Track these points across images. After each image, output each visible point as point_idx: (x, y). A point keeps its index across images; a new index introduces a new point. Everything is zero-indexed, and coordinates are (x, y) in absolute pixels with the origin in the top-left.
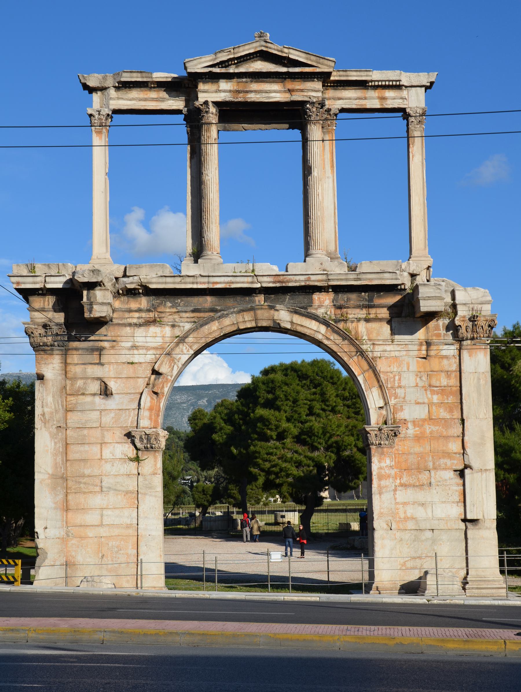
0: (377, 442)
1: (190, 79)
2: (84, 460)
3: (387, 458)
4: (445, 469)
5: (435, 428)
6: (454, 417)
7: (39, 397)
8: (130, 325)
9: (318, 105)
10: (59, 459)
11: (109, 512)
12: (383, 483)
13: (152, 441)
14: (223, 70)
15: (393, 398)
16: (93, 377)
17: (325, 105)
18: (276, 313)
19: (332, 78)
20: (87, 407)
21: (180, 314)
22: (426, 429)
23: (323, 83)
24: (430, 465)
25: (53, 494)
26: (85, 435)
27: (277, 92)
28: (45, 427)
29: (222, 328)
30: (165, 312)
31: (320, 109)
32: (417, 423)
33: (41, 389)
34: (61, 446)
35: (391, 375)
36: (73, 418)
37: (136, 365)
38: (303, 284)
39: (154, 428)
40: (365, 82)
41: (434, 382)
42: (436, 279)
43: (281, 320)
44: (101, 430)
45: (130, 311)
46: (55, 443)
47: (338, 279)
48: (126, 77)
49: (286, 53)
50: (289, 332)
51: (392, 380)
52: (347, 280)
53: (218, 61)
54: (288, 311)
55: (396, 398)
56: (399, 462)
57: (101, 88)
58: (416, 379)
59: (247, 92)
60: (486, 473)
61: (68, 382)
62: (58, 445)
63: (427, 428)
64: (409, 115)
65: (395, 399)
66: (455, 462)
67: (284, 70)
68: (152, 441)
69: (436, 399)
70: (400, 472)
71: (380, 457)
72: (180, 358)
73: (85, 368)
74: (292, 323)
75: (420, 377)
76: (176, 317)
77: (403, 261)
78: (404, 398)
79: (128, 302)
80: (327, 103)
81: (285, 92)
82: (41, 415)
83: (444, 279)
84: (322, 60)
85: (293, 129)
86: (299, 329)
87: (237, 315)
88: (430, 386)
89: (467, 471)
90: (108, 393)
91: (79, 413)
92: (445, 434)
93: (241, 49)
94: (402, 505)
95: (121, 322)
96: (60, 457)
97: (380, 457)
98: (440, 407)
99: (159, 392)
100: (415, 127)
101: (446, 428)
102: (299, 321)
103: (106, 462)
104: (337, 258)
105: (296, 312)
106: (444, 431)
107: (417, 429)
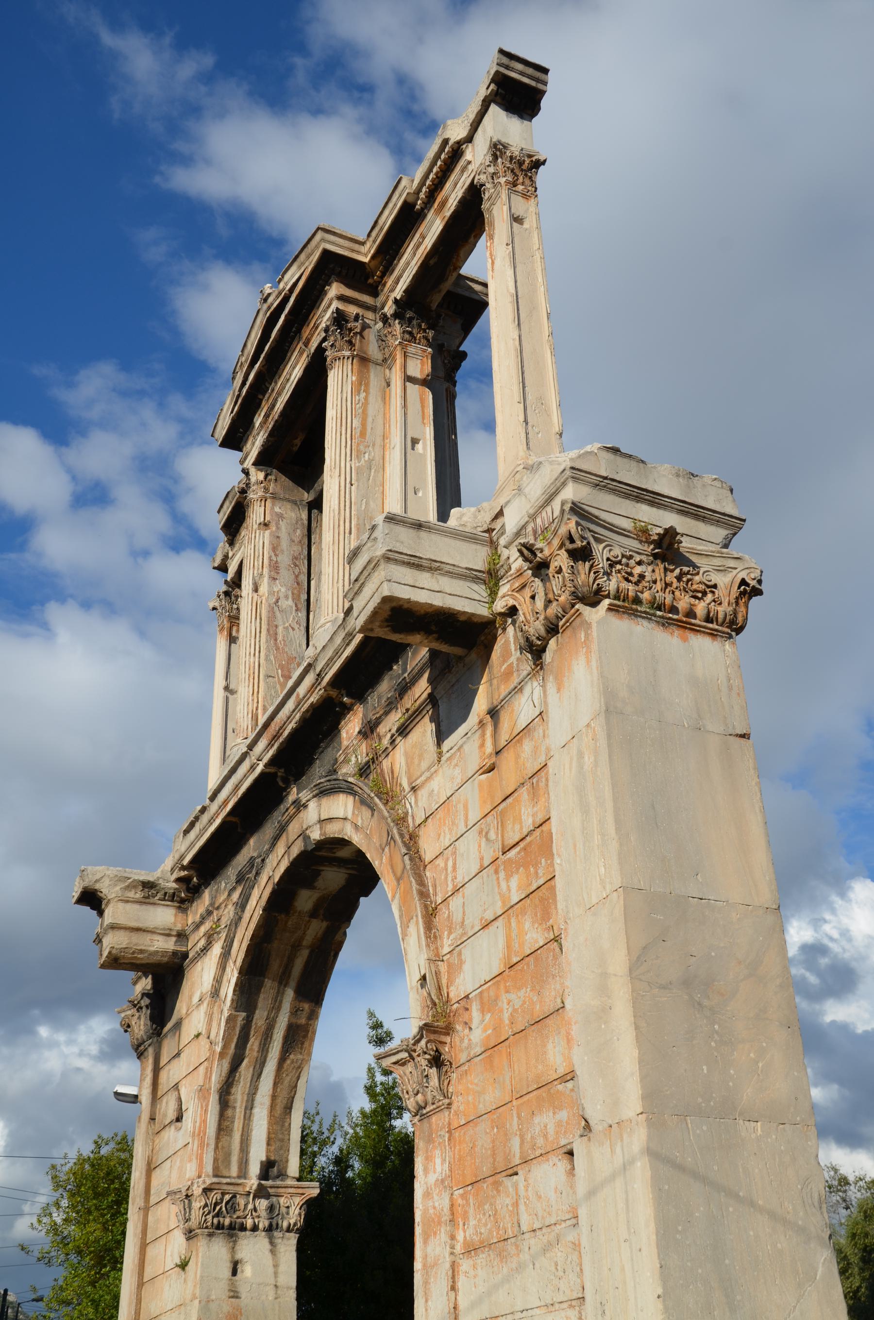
12: (429, 1249)
15: (446, 933)
38: (298, 717)
56: (459, 1160)
58: (480, 846)
66: (563, 1115)
78: (463, 923)
98: (523, 912)
106: (535, 999)
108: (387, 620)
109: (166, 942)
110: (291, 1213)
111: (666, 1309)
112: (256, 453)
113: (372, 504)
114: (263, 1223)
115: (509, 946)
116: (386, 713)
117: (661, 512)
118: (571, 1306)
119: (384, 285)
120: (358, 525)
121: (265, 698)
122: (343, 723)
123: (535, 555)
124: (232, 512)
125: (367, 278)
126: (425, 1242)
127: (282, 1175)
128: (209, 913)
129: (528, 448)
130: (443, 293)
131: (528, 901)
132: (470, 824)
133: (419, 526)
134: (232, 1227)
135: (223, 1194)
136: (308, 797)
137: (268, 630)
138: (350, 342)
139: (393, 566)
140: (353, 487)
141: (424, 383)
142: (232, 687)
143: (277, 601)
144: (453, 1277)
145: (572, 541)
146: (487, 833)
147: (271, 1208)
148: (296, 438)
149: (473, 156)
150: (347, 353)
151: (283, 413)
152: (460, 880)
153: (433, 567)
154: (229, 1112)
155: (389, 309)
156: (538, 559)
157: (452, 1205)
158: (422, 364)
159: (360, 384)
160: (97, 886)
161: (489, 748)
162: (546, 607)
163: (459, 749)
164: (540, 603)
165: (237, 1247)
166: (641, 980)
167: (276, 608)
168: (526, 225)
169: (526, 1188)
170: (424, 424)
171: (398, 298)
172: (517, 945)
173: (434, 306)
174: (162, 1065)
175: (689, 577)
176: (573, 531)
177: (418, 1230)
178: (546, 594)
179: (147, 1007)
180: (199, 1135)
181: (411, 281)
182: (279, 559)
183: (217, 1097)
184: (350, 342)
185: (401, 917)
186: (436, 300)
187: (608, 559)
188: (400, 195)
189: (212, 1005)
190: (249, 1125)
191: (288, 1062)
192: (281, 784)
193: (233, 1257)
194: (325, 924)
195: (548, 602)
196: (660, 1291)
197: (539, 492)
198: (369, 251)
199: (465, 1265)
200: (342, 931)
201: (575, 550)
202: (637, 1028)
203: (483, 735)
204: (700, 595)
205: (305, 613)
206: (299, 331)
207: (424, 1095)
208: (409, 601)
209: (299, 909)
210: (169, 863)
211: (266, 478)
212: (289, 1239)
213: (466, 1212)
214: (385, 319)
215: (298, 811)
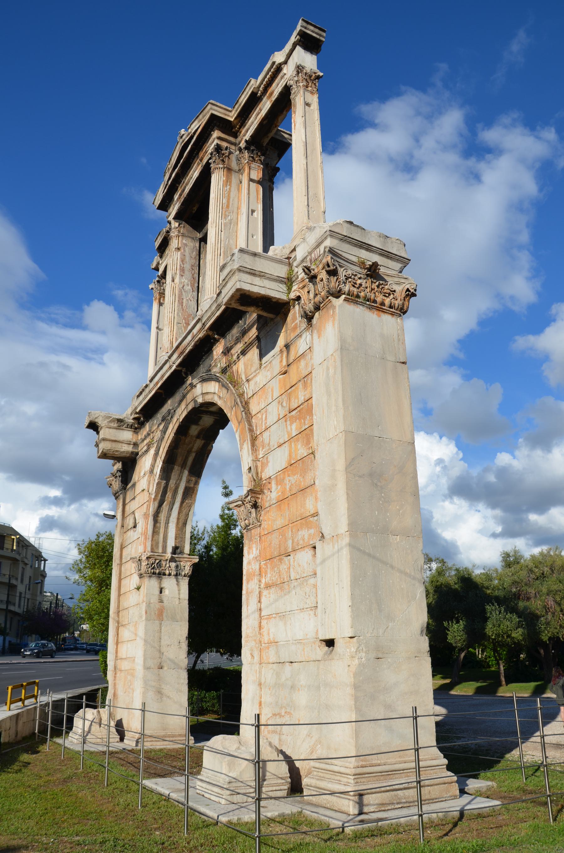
12: (249, 586)
15: (261, 448)
48: (157, 244)
54: (200, 382)
56: (264, 549)
58: (278, 409)
66: (312, 531)
78: (269, 444)
98: (298, 440)
108: (238, 300)
109: (128, 447)
110: (186, 569)
111: (352, 611)
112: (175, 213)
113: (231, 241)
114: (173, 573)
115: (290, 455)
116: (236, 344)
117: (371, 254)
118: (311, 610)
119: (241, 133)
120: (224, 251)
121: (176, 334)
122: (214, 347)
123: (311, 272)
124: (162, 242)
125: (232, 129)
126: (248, 583)
127: (182, 552)
128: (149, 435)
129: (309, 219)
130: (269, 138)
131: (300, 435)
132: (274, 398)
133: (255, 255)
134: (159, 574)
135: (156, 560)
136: (197, 382)
137: (179, 301)
138: (223, 161)
139: (242, 274)
140: (222, 233)
141: (259, 182)
142: (160, 327)
143: (183, 287)
144: (260, 597)
145: (328, 266)
146: (282, 403)
147: (177, 567)
148: (194, 207)
149: (287, 71)
150: (221, 166)
151: (189, 194)
152: (268, 424)
153: (261, 275)
154: (158, 525)
155: (243, 145)
156: (312, 274)
157: (260, 568)
158: (258, 173)
159: (227, 182)
160: (96, 420)
161: (284, 363)
162: (315, 297)
163: (270, 363)
164: (312, 295)
165: (162, 582)
166: (350, 473)
167: (183, 290)
168: (312, 107)
169: (294, 561)
170: (258, 203)
171: (247, 139)
173: (265, 144)
174: (126, 503)
175: (383, 286)
176: (329, 262)
177: (244, 578)
178: (315, 291)
179: (119, 476)
180: (144, 534)
181: (254, 132)
182: (185, 266)
183: (152, 518)
184: (223, 161)
185: (240, 440)
186: (266, 141)
187: (345, 276)
188: (250, 88)
189: (150, 477)
190: (167, 531)
191: (185, 503)
192: (184, 375)
193: (160, 586)
194: (203, 442)
195: (316, 295)
196: (350, 604)
197: (314, 241)
198: (234, 115)
199: (265, 593)
200: (211, 445)
201: (330, 270)
202: (348, 494)
203: (282, 357)
204: (387, 295)
205: (196, 293)
206: (198, 154)
207: (249, 520)
208: (249, 291)
209: (191, 434)
210: (129, 411)
211: (179, 226)
212: (185, 580)
213: (266, 571)
214: (240, 150)
215: (192, 388)
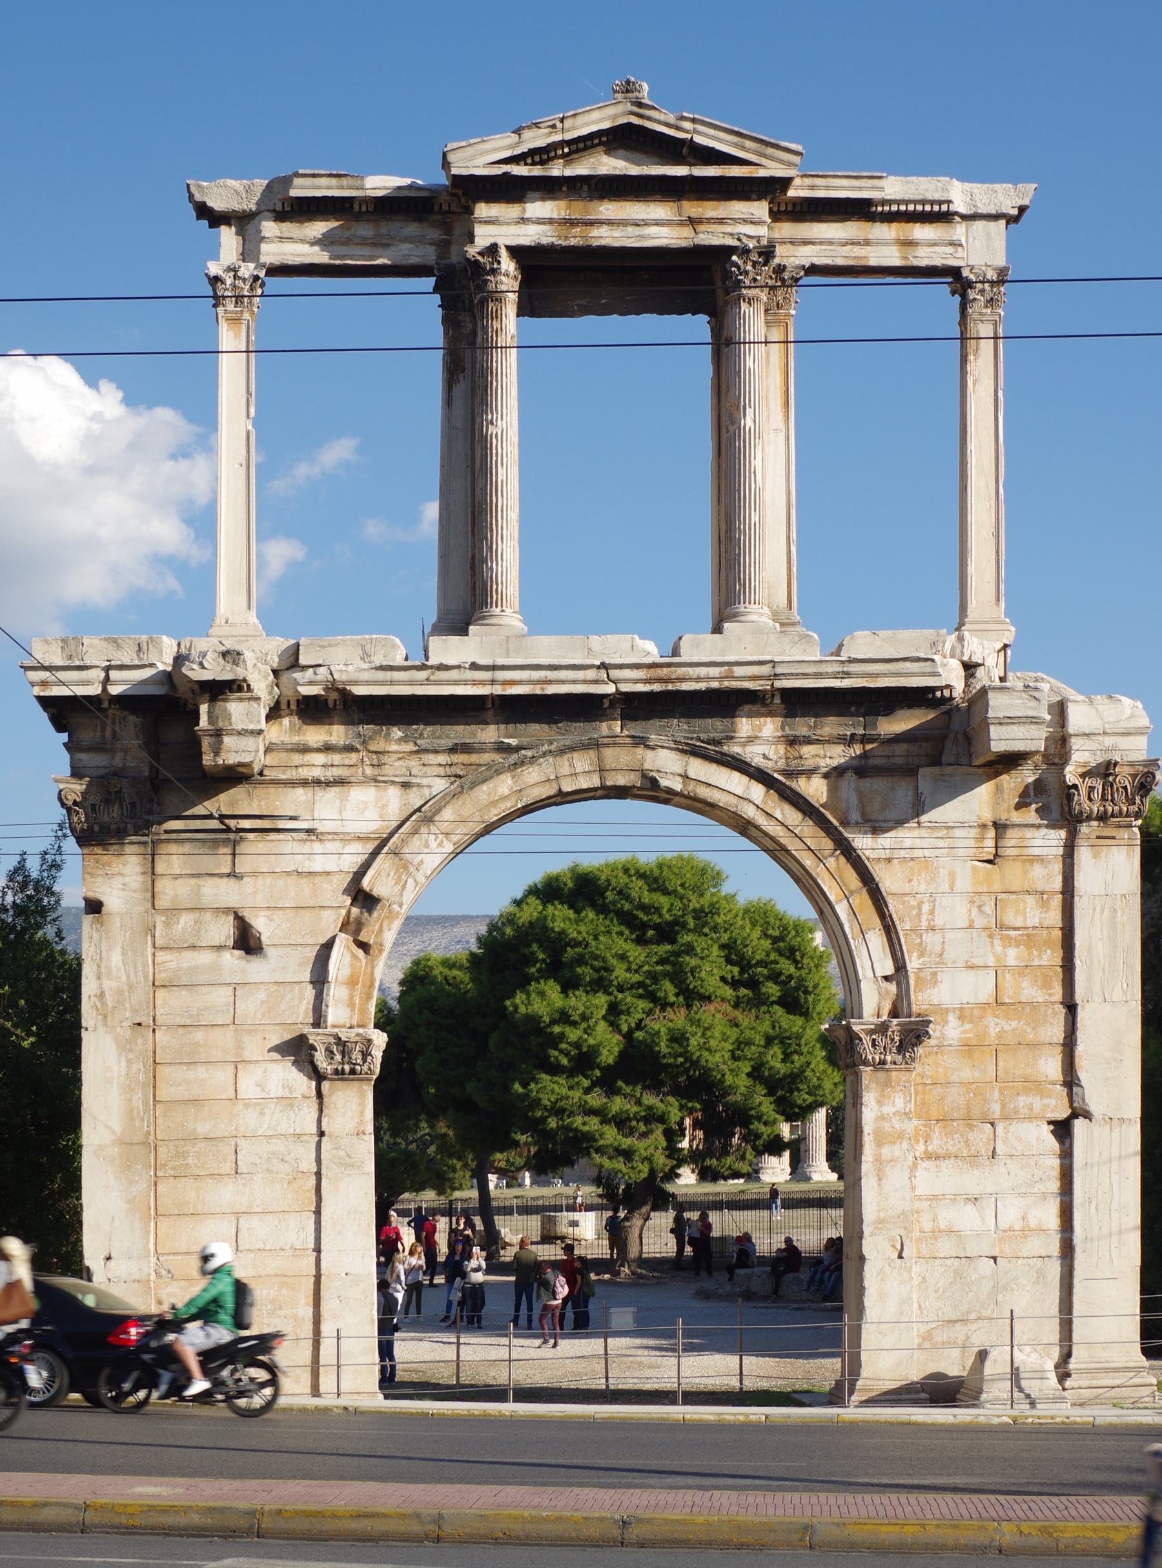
0: (877, 1058)
1: (455, 191)
2: (195, 1102)
3: (897, 1095)
4: (1029, 1118)
5: (1010, 1025)
6: (1053, 999)
7: (90, 955)
8: (304, 783)
9: (756, 256)
10: (137, 1100)
11: (254, 1222)
12: (886, 1151)
13: (353, 1057)
14: (537, 171)
15: (915, 954)
16: (217, 906)
17: (774, 257)
18: (649, 754)
19: (791, 193)
20: (202, 979)
21: (423, 756)
22: (988, 1027)
23: (770, 203)
24: (996, 1109)
25: (124, 1181)
26: (197, 1044)
27: (662, 225)
28: (106, 1025)
29: (520, 791)
30: (388, 752)
31: (764, 265)
32: (968, 1012)
33: (95, 935)
34: (142, 1068)
35: (913, 902)
36: (169, 1004)
37: (318, 879)
39: (359, 1026)
40: (868, 202)
41: (1011, 918)
42: (1019, 674)
43: (659, 771)
44: (236, 1031)
45: (305, 749)
46: (129, 1062)
47: (797, 675)
49: (687, 132)
50: (677, 799)
51: (914, 913)
52: (818, 675)
53: (524, 148)
55: (921, 955)
56: (924, 1103)
57: (239, 215)
59: (591, 223)
60: (1121, 1126)
61: (160, 920)
62: (135, 1067)
63: (992, 1025)
64: (969, 284)
65: (919, 959)
66: (1052, 1102)
67: (681, 171)
68: (357, 1056)
69: (1013, 956)
70: (925, 1126)
71: (883, 1091)
72: (422, 861)
73: (199, 886)
74: (685, 777)
75: (980, 907)
76: (414, 763)
77: (949, 633)
78: (941, 955)
79: (299, 729)
80: (779, 250)
81: (681, 224)
82: (95, 996)
83: (1039, 674)
84: (770, 151)
85: (693, 315)
86: (703, 792)
87: (558, 758)
88: (1002, 927)
89: (1079, 1124)
90: (252, 943)
91: (183, 993)
92: (1031, 1037)
93: (580, 120)
94: (929, 1203)
95: (284, 777)
96: (140, 1095)
97: (883, 1091)
98: (1022, 975)
99: (371, 942)
100: (981, 314)
101: (1032, 1025)
102: (702, 773)
103: (247, 1106)
104: (793, 624)
105: (694, 752)
106: (1029, 1031)
107: (968, 1026)
172: (1011, 993)
